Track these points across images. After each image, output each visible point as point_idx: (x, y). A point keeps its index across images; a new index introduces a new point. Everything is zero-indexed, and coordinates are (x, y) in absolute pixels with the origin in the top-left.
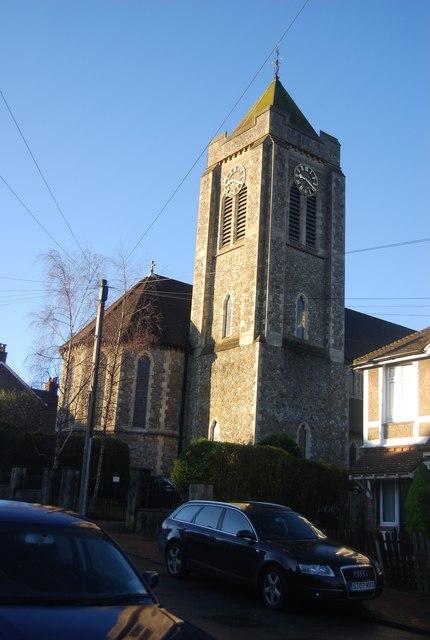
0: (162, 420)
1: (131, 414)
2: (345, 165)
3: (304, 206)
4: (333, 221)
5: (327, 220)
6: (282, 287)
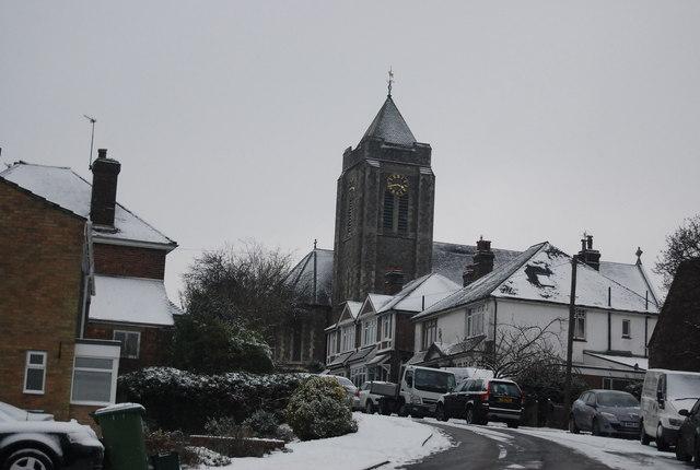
0: (311, 355)
1: (291, 352)
3: (396, 205)
4: (420, 211)
6: (374, 266)
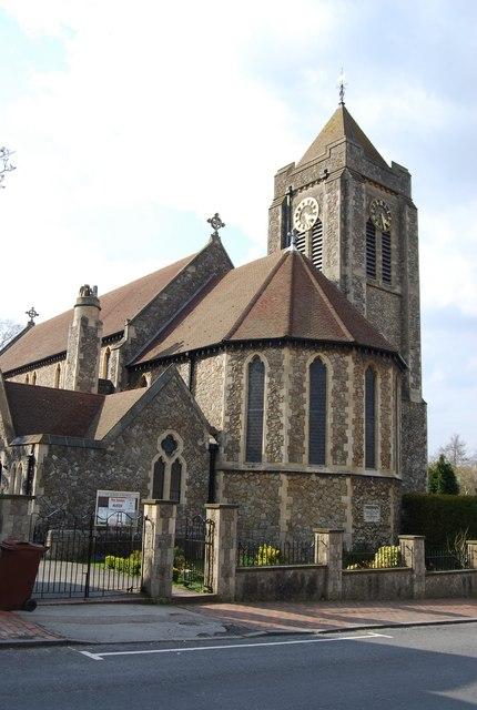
2: (417, 195)
5: (402, 260)
